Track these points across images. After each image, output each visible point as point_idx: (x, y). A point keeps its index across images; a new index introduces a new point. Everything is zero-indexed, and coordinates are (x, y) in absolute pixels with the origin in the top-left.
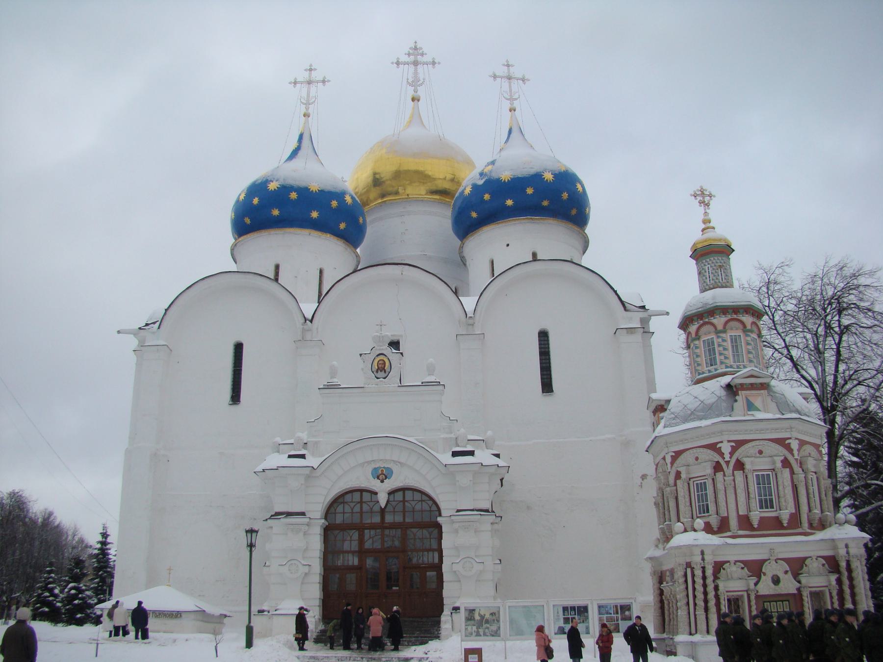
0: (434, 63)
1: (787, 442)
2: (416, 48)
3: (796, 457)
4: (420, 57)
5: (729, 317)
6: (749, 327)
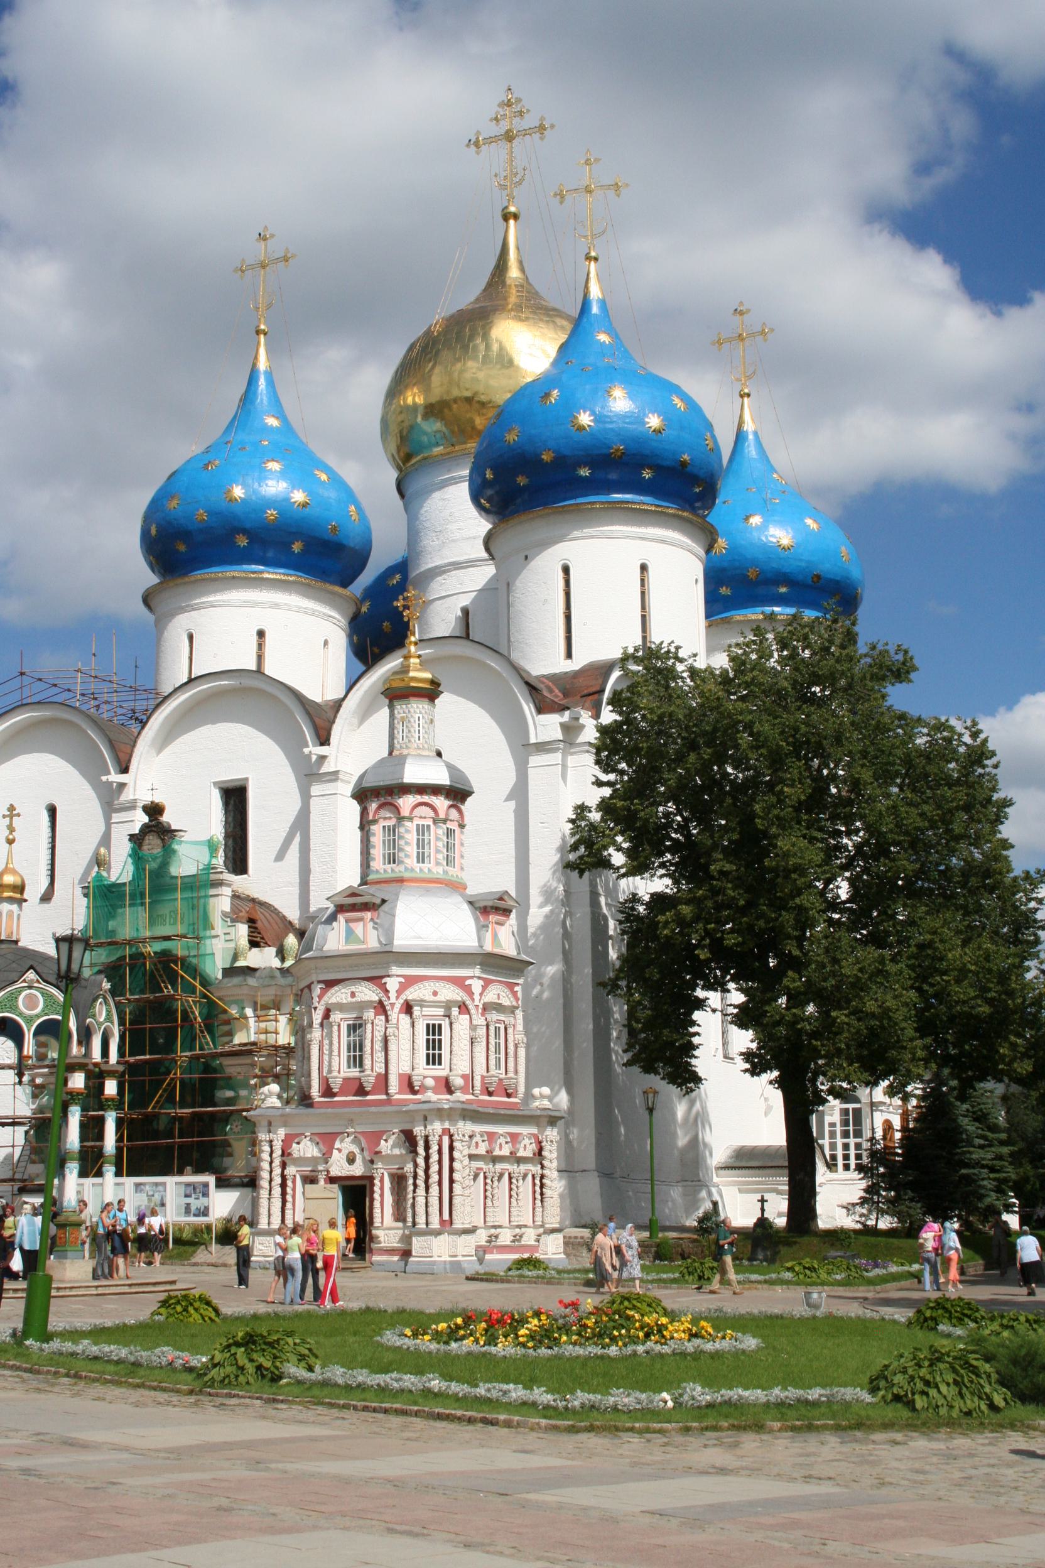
0: (541, 128)
1: (384, 981)
2: (509, 104)
3: (393, 1000)
4: (518, 119)
5: (382, 800)
6: (405, 812)
